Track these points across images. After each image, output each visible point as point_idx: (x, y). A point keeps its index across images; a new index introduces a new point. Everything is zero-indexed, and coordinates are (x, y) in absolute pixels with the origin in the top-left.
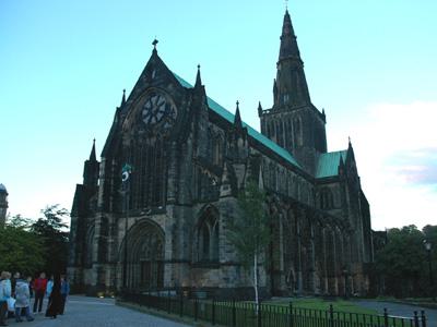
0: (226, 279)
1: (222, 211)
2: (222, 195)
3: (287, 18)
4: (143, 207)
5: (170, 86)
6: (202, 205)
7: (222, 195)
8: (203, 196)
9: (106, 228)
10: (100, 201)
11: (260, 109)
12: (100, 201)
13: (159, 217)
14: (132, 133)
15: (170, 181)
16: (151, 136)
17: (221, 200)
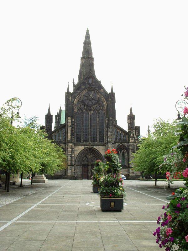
0: (133, 173)
1: (131, 147)
2: (130, 142)
3: (88, 33)
4: (86, 141)
5: (102, 90)
6: (118, 144)
7: (130, 142)
8: (118, 140)
9: (73, 150)
10: (69, 138)
11: (73, 82)
12: (69, 138)
13: (98, 147)
14: (79, 106)
15: (109, 133)
16: (90, 110)
17: (130, 143)
